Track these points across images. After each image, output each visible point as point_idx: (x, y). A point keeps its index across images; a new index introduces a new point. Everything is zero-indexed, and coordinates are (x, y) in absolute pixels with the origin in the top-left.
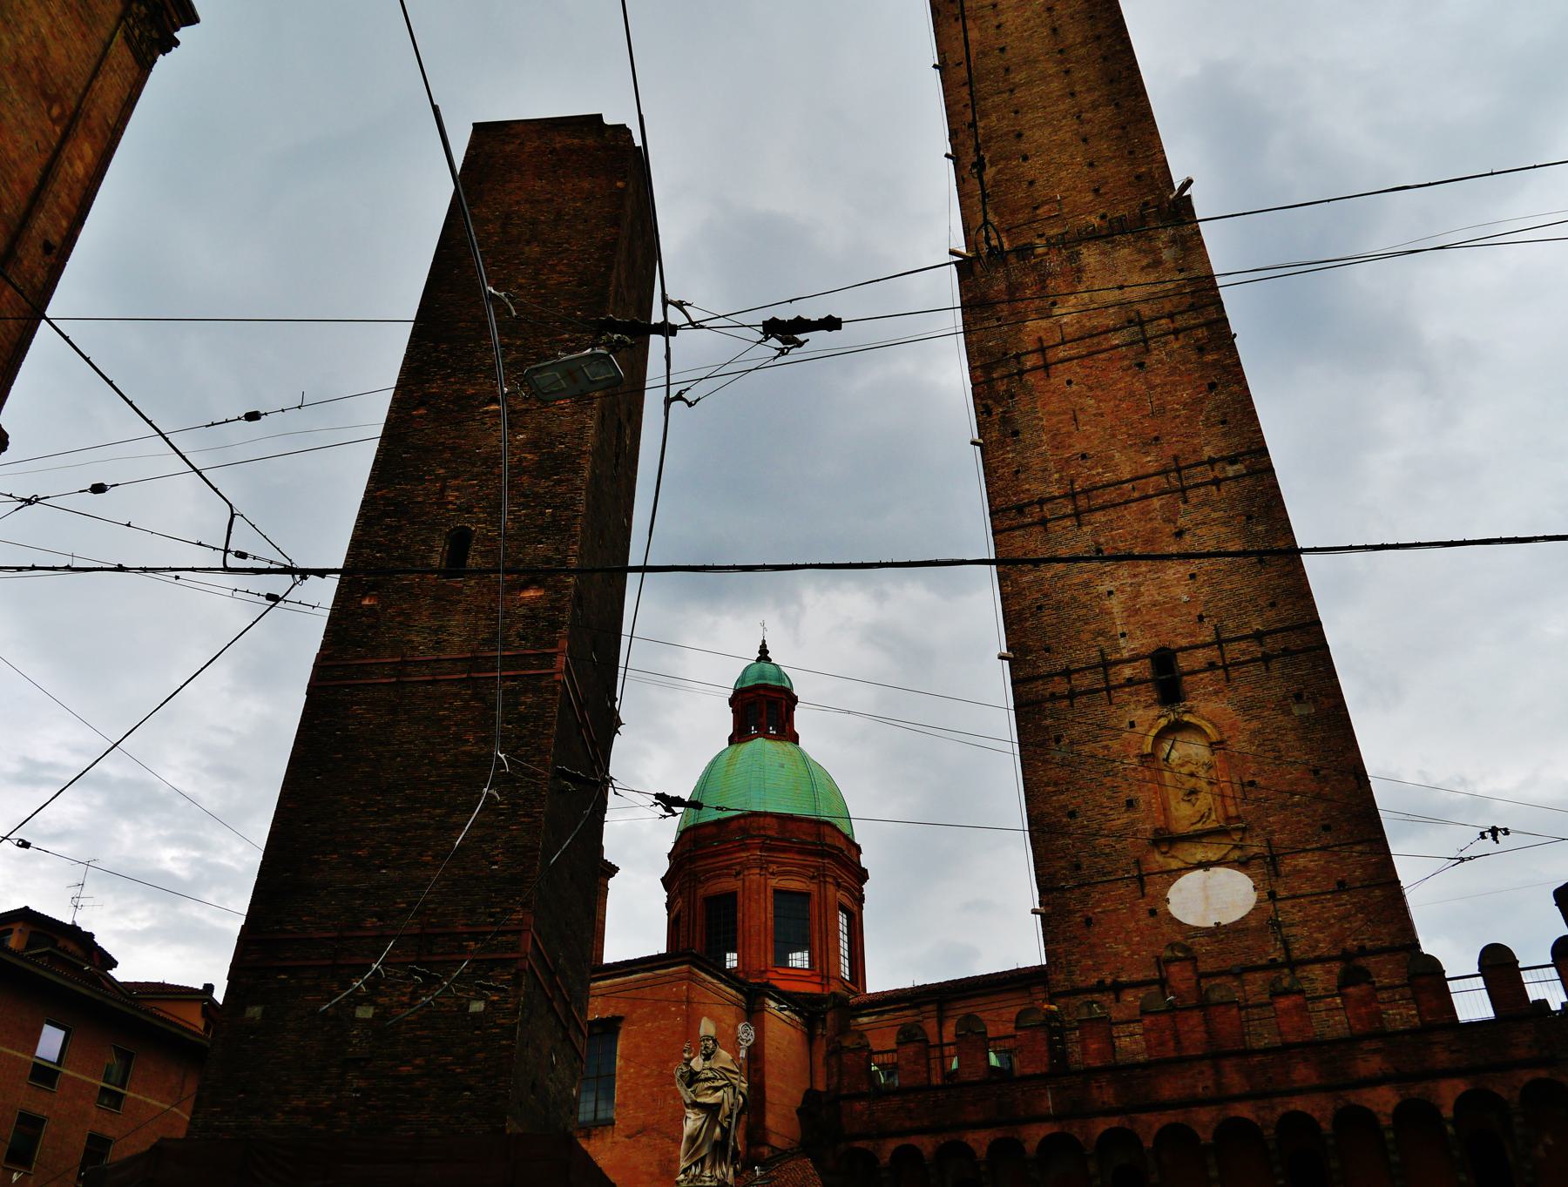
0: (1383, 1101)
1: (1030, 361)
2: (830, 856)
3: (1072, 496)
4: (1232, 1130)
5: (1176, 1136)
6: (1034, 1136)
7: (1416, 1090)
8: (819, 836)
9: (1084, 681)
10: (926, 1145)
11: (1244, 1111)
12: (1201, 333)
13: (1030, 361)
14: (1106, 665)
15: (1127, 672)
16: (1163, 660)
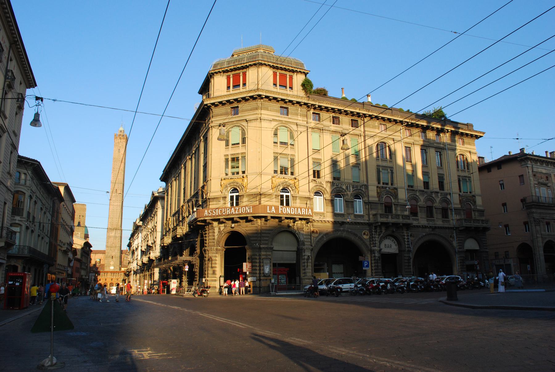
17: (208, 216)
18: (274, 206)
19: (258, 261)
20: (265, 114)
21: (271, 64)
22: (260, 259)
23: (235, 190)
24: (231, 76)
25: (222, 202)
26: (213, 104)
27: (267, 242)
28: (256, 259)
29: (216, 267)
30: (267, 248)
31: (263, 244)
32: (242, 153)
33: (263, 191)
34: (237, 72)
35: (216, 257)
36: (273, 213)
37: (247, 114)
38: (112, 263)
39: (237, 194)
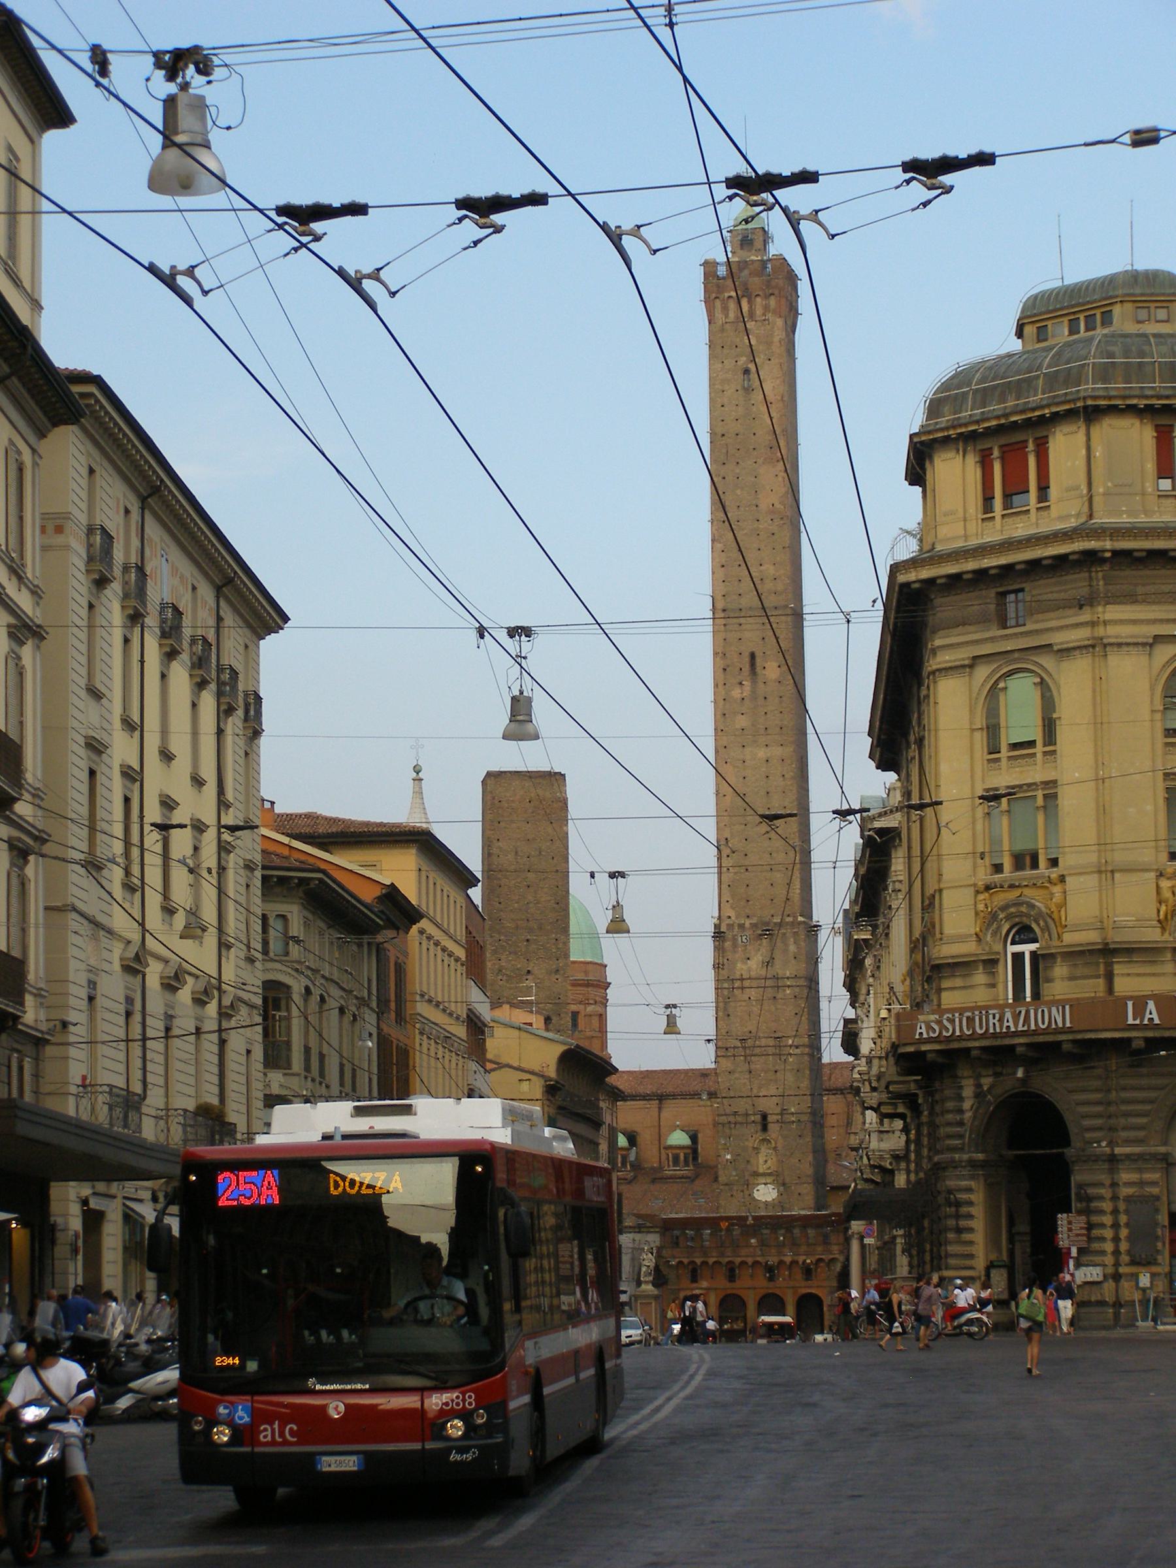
0: (788, 1259)
1: (737, 984)
2: (593, 985)
3: (744, 1048)
4: (756, 1263)
5: (743, 1263)
6: (711, 1261)
7: (796, 1258)
8: (586, 973)
9: (739, 1119)
10: (686, 1261)
11: (759, 1259)
12: (797, 990)
13: (737, 984)
14: (747, 1115)
15: (753, 1118)
16: (764, 1117)
17: (930, 1040)
18: (1155, 997)
19: (1107, 1206)
20: (1122, 622)
21: (1142, 403)
22: (1115, 1198)
23: (1024, 933)
24: (996, 453)
25: (980, 977)
26: (931, 582)
27: (1141, 1134)
28: (1101, 1198)
29: (971, 1230)
30: (1139, 1157)
31: (1128, 1142)
32: (1046, 783)
33: (1117, 938)
34: (1018, 437)
35: (969, 1190)
36: (1151, 1026)
37: (1053, 624)
38: (764, 1161)
39: (1033, 947)
